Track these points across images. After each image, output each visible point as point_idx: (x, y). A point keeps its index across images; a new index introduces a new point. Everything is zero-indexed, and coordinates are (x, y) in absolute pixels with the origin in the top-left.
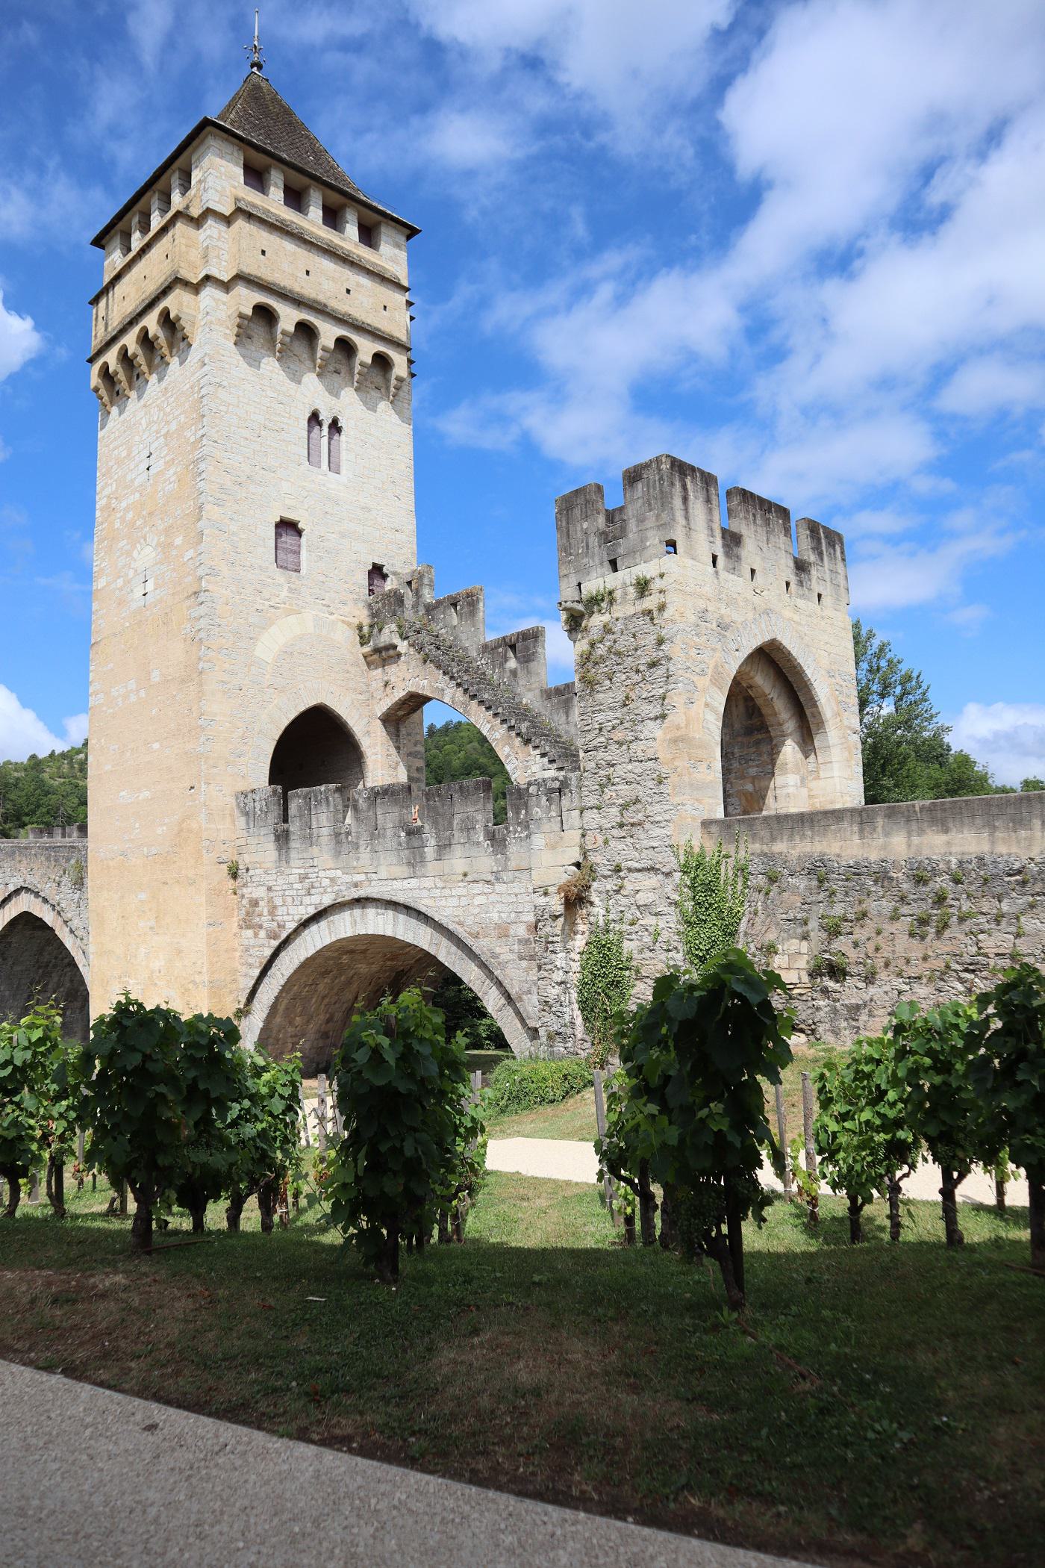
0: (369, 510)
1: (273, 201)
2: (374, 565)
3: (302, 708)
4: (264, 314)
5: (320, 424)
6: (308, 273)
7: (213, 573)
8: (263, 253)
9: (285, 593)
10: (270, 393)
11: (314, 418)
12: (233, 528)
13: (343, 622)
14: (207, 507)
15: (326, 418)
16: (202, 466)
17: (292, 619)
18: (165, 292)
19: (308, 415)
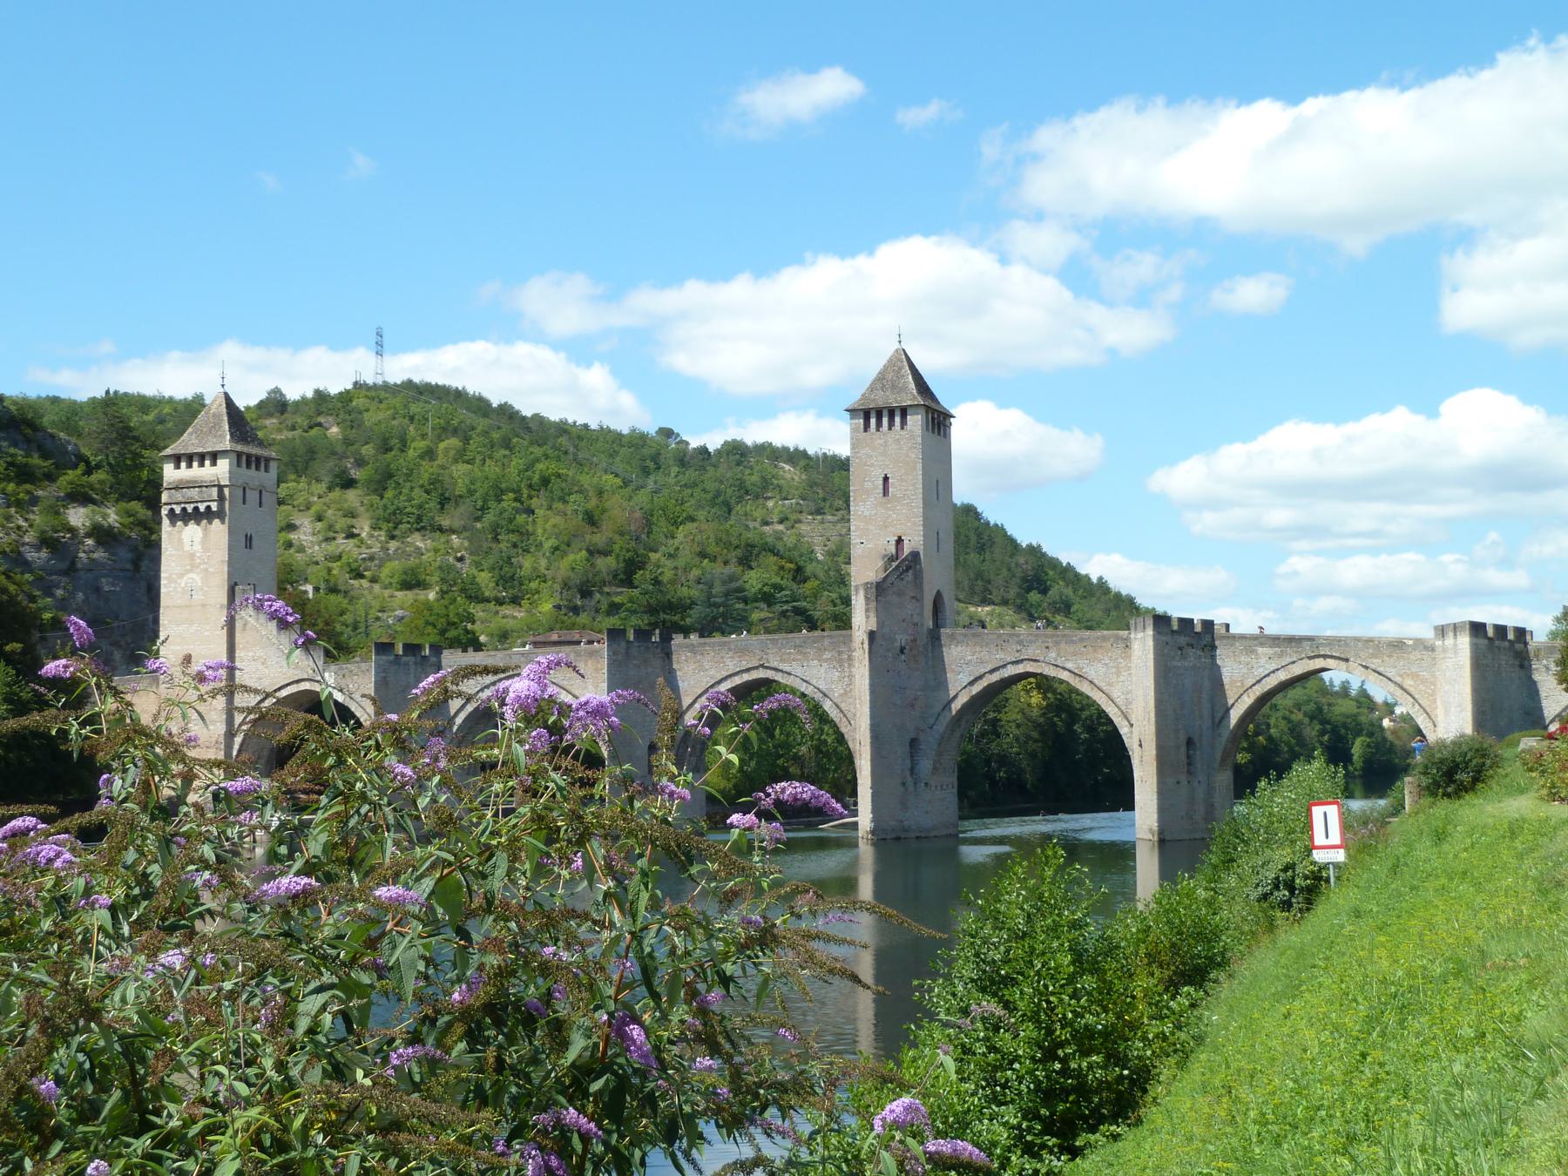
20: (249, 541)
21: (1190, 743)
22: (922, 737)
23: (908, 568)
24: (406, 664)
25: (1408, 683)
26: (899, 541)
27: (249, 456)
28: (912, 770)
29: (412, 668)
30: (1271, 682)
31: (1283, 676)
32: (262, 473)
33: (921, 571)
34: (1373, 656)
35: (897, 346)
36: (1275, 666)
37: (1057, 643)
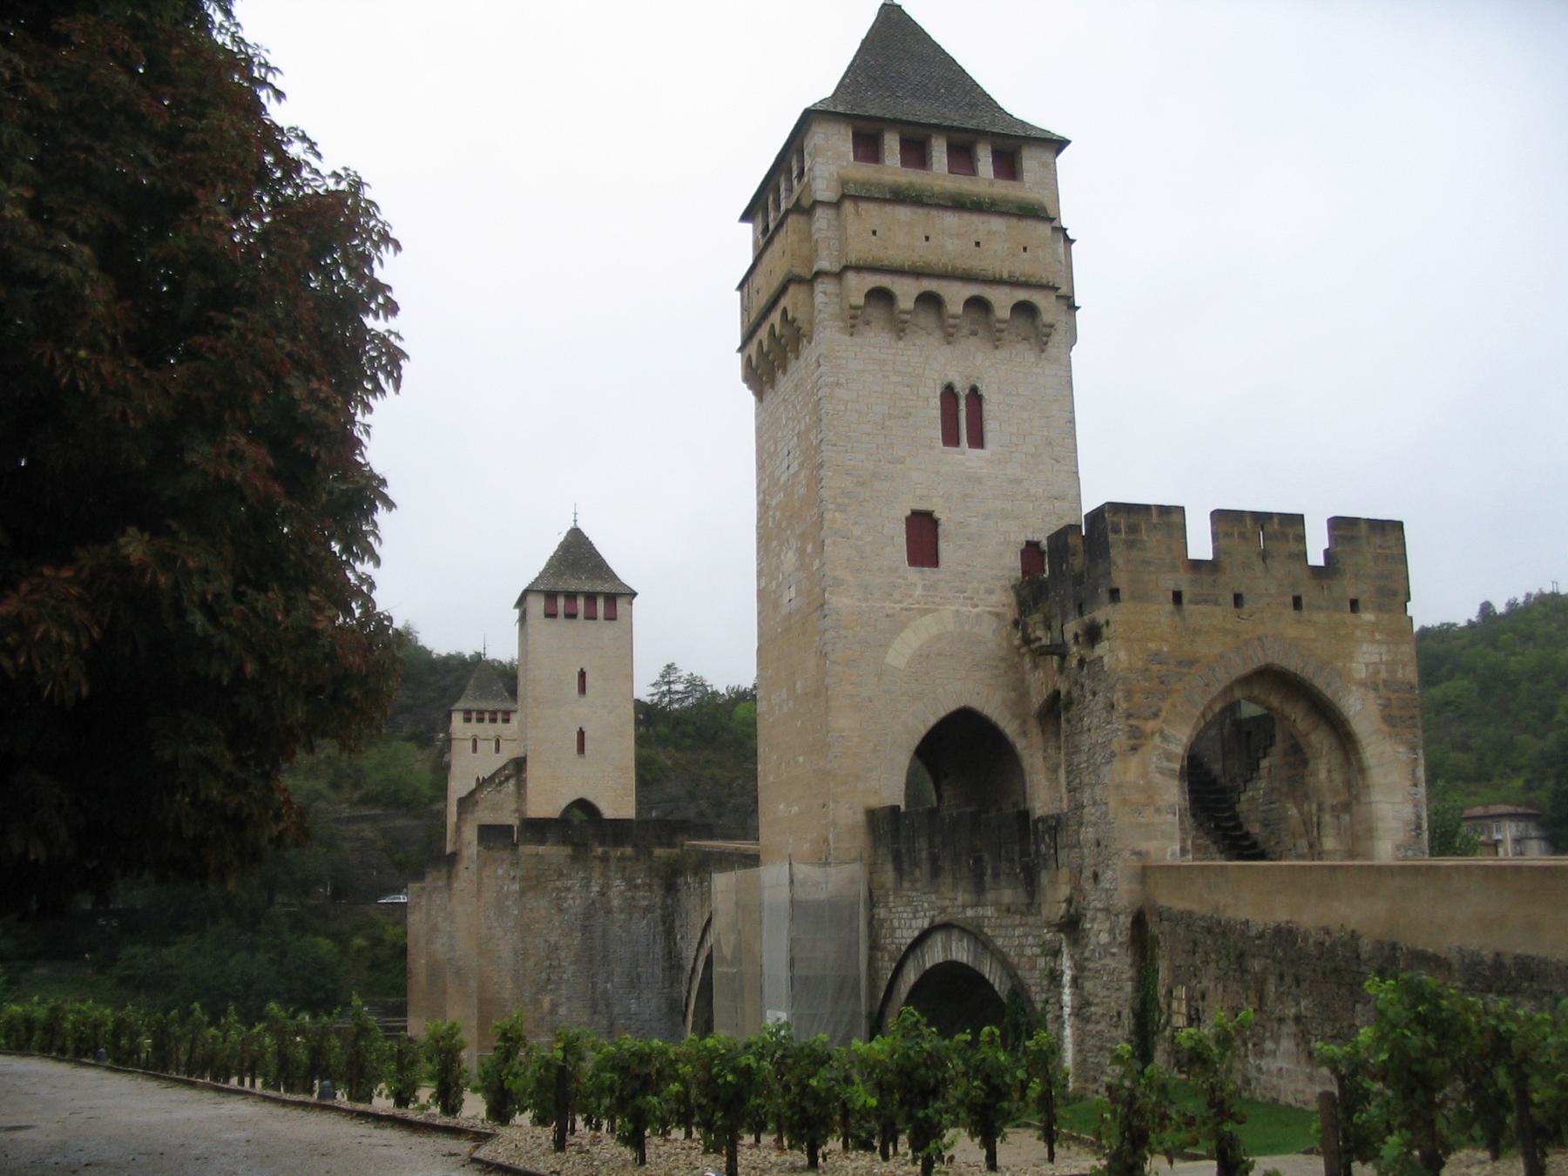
0: (1018, 481)
1: (892, 167)
2: (1029, 543)
3: (942, 714)
4: (881, 296)
5: (956, 397)
6: (927, 238)
7: (838, 582)
8: (874, 233)
9: (918, 592)
10: (894, 379)
11: (949, 394)
12: (857, 531)
13: (990, 613)
14: (828, 516)
15: (962, 390)
16: (822, 472)
17: (928, 619)
18: (782, 290)
19: (938, 393)
23: (507, 778)
27: (481, 712)
32: (500, 725)
33: (525, 780)
35: (572, 524)
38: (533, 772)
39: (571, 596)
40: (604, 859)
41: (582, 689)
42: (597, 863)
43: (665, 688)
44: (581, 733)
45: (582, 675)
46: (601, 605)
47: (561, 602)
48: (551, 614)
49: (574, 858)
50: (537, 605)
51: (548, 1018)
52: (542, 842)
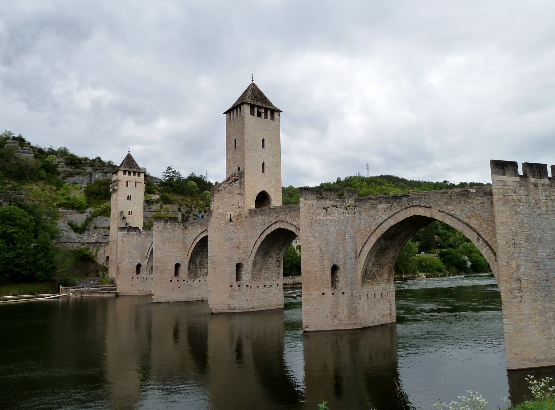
20: (129, 198)
21: (335, 269)
22: (244, 263)
23: (235, 181)
24: (132, 235)
25: (473, 222)
26: (239, 168)
28: (238, 278)
29: (135, 236)
30: (386, 227)
31: (392, 222)
33: (244, 181)
34: (447, 203)
35: (251, 82)
36: (387, 216)
37: (290, 211)
38: (248, 178)
39: (259, 107)
40: (536, 185)
41: (263, 147)
42: (532, 186)
43: (168, 174)
44: (263, 164)
45: (263, 140)
46: (269, 113)
47: (256, 109)
48: (252, 114)
49: (521, 184)
50: (247, 109)
51: (515, 274)
52: (504, 174)
